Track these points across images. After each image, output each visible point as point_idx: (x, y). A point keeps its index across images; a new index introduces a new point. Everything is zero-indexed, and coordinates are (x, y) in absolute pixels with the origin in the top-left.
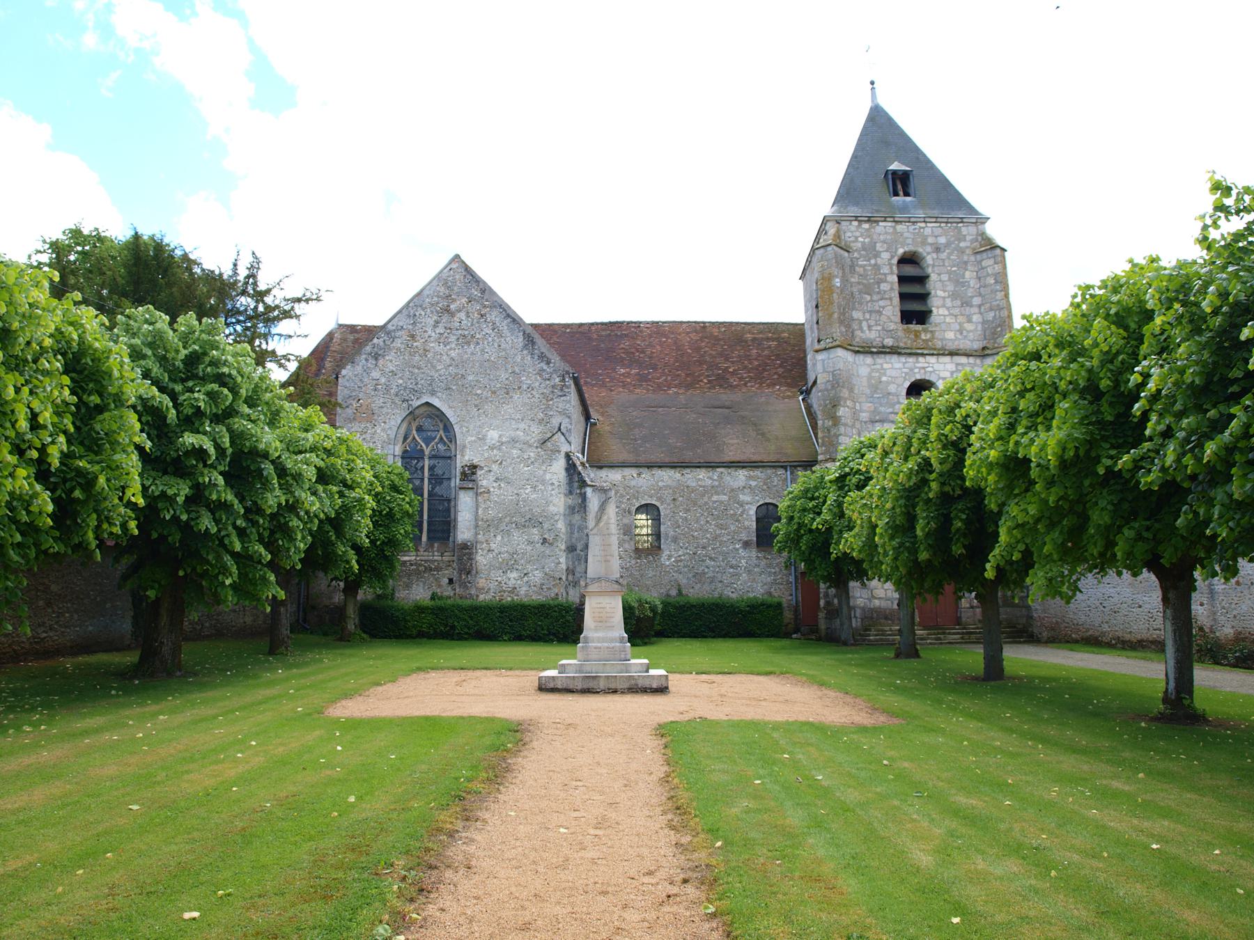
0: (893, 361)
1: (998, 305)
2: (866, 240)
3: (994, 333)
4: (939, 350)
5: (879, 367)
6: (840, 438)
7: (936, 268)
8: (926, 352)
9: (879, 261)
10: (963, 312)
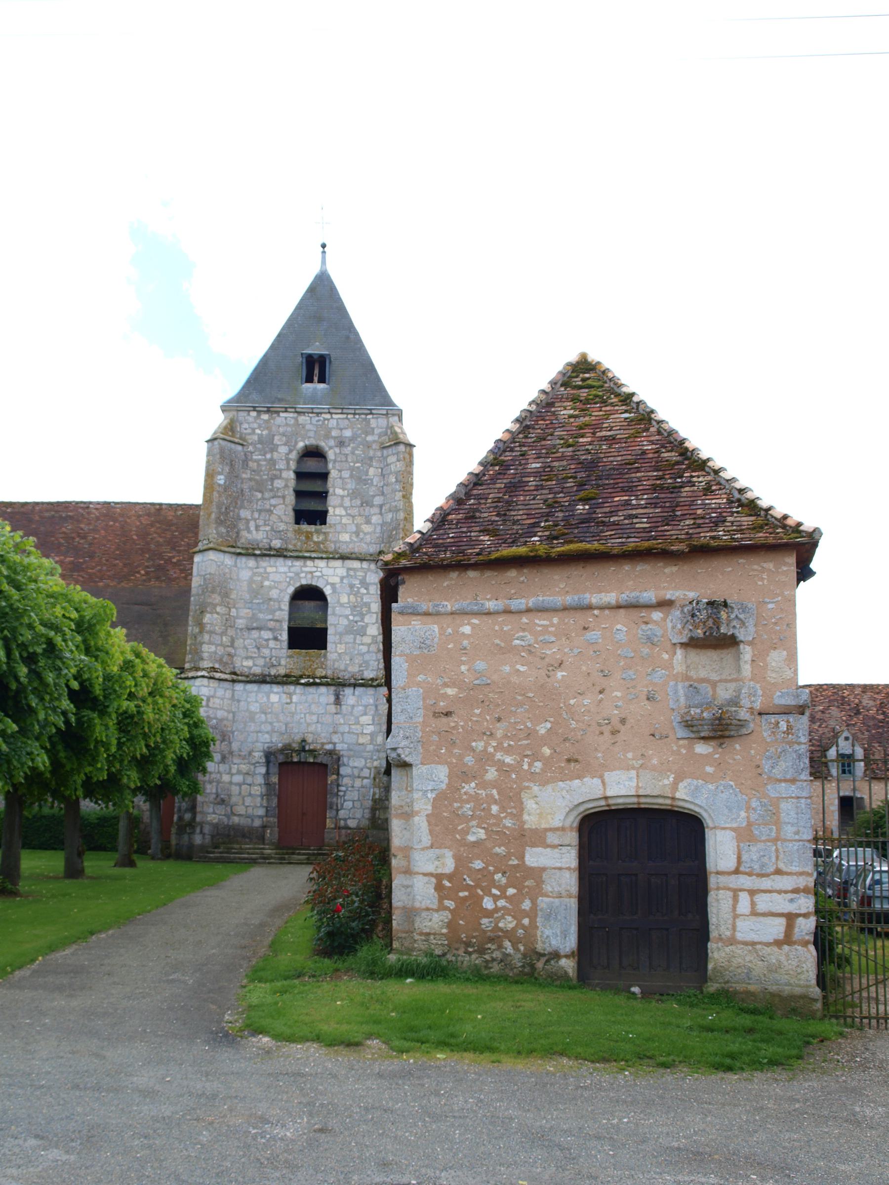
0: (278, 564)
1: (396, 506)
2: (264, 433)
3: (390, 537)
4: (331, 553)
5: (261, 570)
6: (204, 646)
7: (337, 464)
8: (313, 555)
9: (275, 455)
10: (362, 513)
